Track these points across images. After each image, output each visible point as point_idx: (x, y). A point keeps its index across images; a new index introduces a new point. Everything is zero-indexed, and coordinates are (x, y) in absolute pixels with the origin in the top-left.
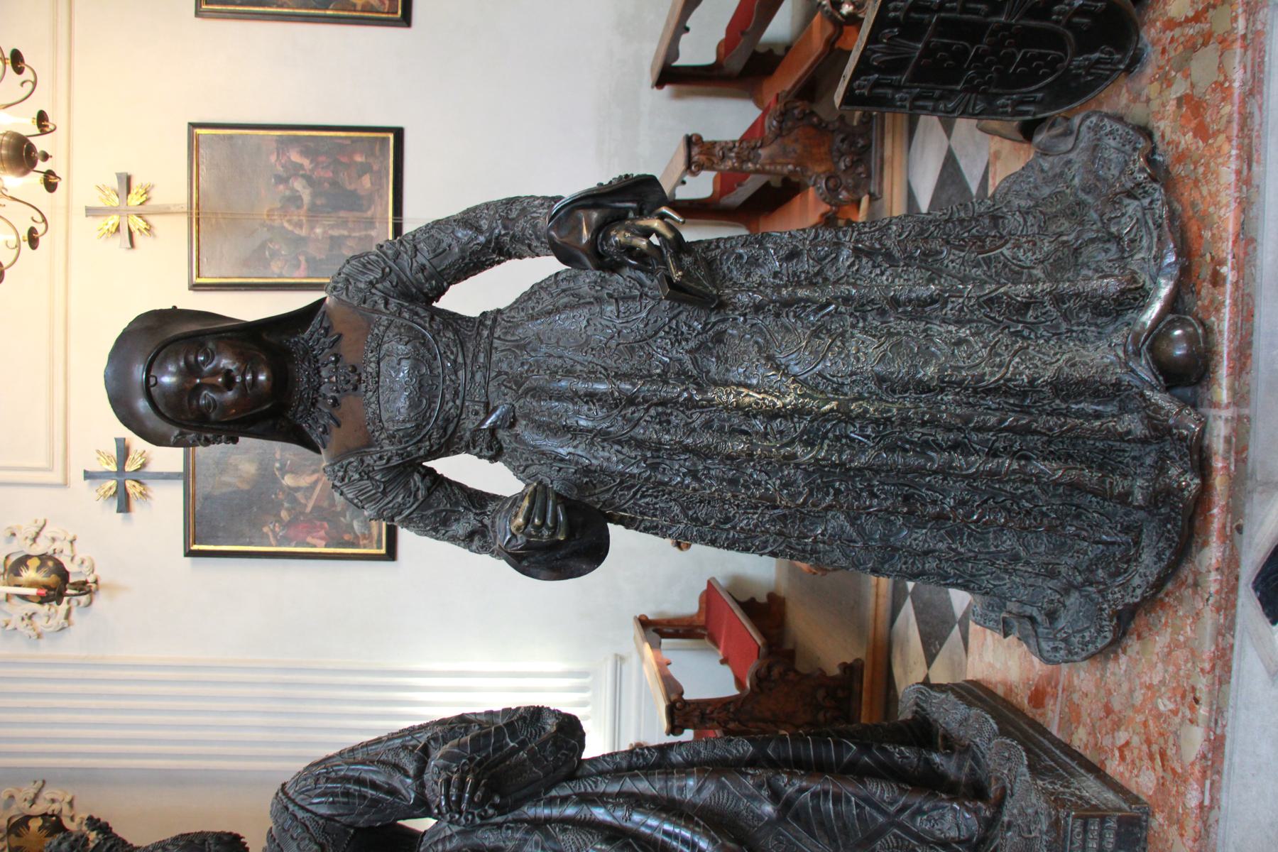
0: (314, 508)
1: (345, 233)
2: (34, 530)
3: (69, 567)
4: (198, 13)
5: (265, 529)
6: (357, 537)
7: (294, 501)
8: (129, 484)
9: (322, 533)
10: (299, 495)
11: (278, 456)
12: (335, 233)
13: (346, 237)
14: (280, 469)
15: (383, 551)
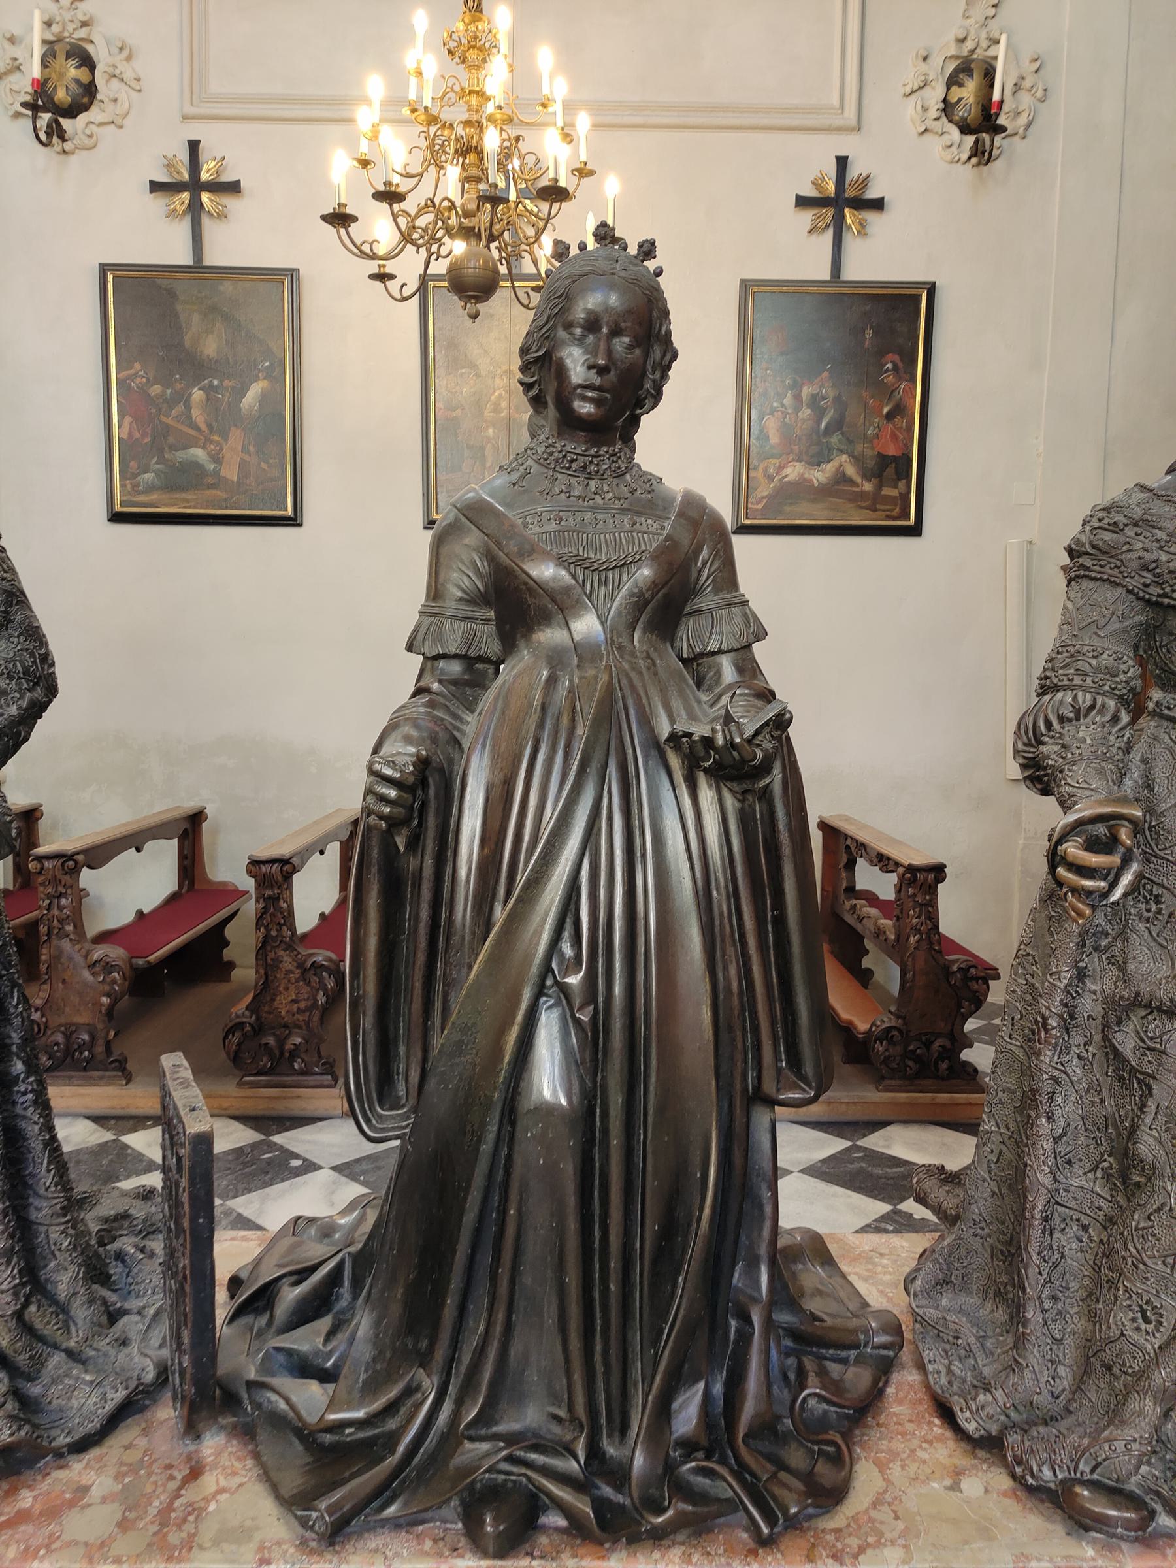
0: (167, 425)
1: (488, 465)
2: (128, 75)
3: (83, 118)
4: (745, 284)
5: (137, 366)
6: (135, 476)
7: (172, 402)
8: (185, 196)
9: (137, 435)
10: (180, 407)
11: (226, 383)
12: (489, 452)
13: (484, 466)
14: (211, 385)
15: (118, 507)
